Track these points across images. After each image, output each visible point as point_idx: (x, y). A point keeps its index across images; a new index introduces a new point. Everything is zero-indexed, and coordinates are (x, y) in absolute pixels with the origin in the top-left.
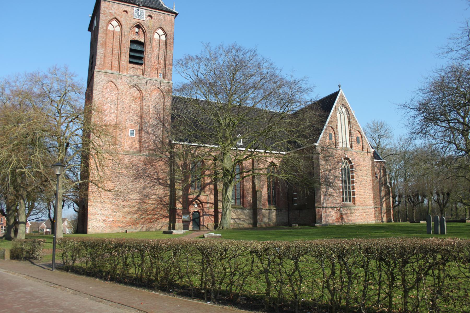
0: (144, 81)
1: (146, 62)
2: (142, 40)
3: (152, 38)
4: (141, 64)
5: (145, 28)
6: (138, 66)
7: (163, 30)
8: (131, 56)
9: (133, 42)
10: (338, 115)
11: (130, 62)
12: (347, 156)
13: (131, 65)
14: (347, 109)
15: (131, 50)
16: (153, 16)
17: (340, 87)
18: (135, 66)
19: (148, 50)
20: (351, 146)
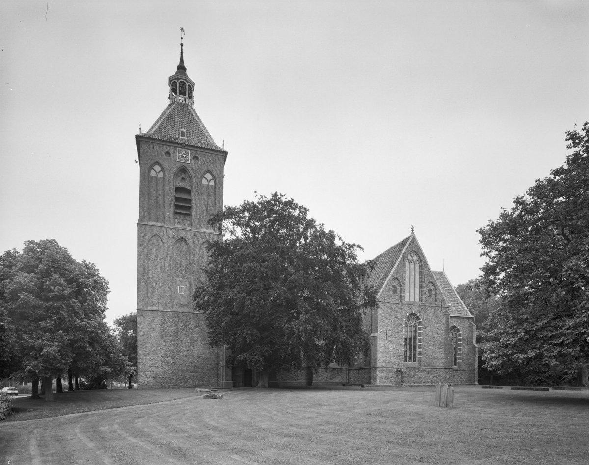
0: (191, 234)
1: (194, 211)
2: (188, 187)
3: (199, 184)
4: (189, 215)
5: (191, 172)
6: (185, 218)
7: (211, 174)
8: (176, 207)
9: (179, 190)
10: (407, 264)
11: (176, 213)
12: (414, 312)
13: (177, 216)
14: (419, 257)
15: (177, 199)
16: (200, 157)
17: (412, 230)
18: (181, 217)
19: (194, 197)
20: (421, 300)
